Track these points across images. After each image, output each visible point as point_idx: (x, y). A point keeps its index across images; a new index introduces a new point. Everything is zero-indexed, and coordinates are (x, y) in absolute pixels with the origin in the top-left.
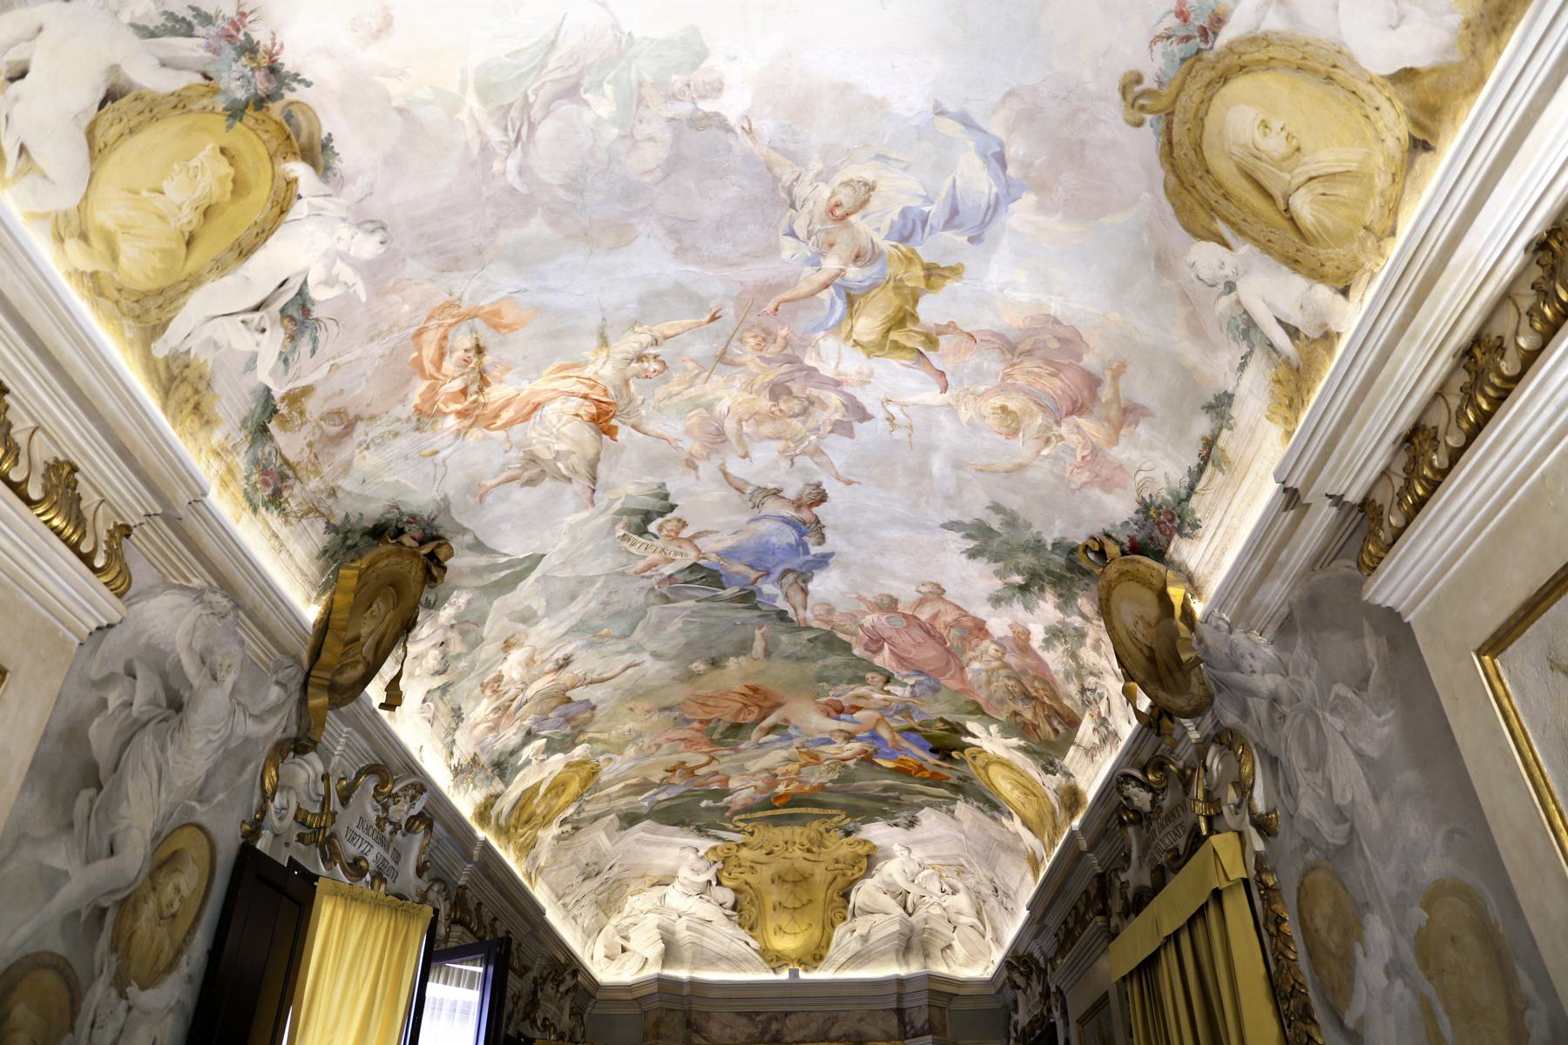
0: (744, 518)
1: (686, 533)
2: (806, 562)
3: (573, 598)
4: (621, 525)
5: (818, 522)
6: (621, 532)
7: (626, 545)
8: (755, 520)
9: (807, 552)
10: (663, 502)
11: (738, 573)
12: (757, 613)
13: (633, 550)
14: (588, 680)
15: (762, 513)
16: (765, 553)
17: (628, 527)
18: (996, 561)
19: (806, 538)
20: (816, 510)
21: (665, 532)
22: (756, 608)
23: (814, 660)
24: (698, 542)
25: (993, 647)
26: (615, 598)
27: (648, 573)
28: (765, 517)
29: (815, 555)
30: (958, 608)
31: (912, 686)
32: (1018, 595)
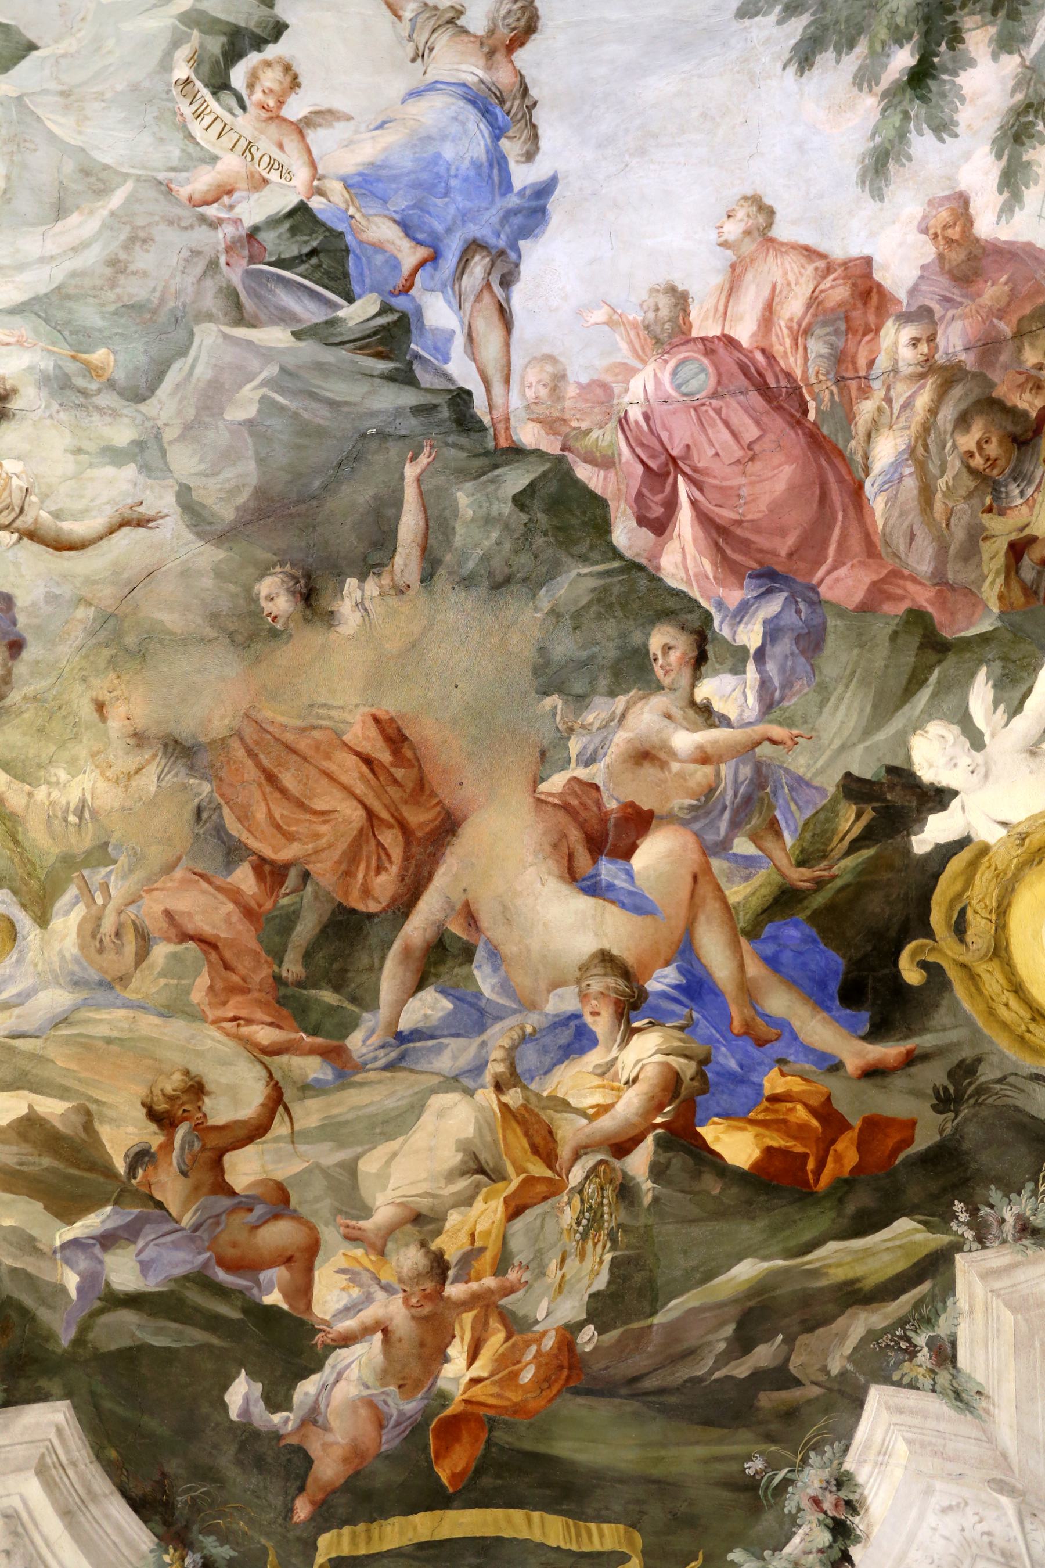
0: (399, 86)
1: (296, 109)
2: (509, 214)
3: (60, 211)
4: (184, 52)
5: (525, 91)
6: (182, 71)
7: (187, 109)
8: (416, 93)
9: (506, 185)
10: (265, 10)
11: (378, 248)
12: (409, 398)
13: (196, 128)
14: (26, 521)
15: (430, 78)
16: (429, 188)
17: (197, 61)
18: (851, 45)
19: (504, 143)
20: (523, 57)
21: (258, 96)
22: (405, 378)
23: (534, 584)
24: (316, 138)
25: (908, 332)
26: (143, 260)
27: (212, 211)
28: (432, 87)
29: (522, 193)
30: (810, 253)
31: (760, 655)
32: (916, 108)
